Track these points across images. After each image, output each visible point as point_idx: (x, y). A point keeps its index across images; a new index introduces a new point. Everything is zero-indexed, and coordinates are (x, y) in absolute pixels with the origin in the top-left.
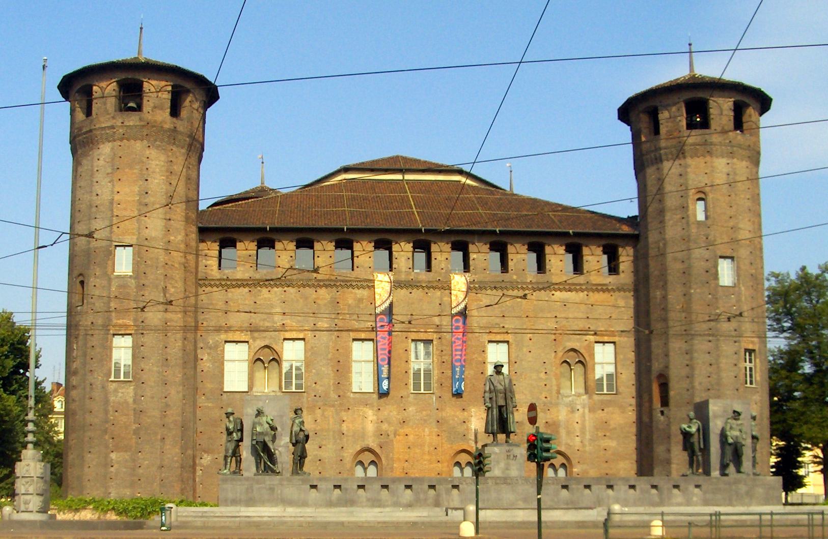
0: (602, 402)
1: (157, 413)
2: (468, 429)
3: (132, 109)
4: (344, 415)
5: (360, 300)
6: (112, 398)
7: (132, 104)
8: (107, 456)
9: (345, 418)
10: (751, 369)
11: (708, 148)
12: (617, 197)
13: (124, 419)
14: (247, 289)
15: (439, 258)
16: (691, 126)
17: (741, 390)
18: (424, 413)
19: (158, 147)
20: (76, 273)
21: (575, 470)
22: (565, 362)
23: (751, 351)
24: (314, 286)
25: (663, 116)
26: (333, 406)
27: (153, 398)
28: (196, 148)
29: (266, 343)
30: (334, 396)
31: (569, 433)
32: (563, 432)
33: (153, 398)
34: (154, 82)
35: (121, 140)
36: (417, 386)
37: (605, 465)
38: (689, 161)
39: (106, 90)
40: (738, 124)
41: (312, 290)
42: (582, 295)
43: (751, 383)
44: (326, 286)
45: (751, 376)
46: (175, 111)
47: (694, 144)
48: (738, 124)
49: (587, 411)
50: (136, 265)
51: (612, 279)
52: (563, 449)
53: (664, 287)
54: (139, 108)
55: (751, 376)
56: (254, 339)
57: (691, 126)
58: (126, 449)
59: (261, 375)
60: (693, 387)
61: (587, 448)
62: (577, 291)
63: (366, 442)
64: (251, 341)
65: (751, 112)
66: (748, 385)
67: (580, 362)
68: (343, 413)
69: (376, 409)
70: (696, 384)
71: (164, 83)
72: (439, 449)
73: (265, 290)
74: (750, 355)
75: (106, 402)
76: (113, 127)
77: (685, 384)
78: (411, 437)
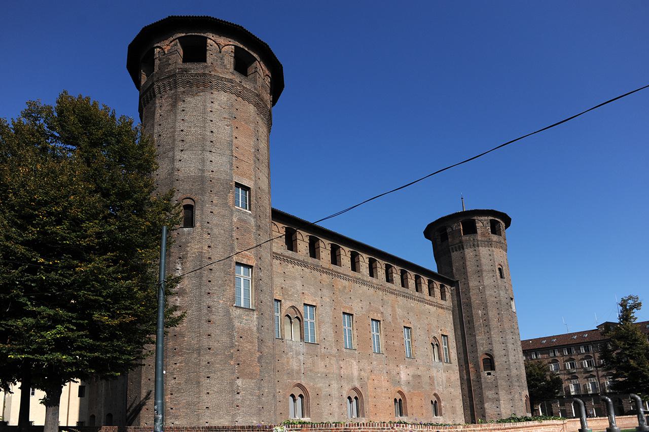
2: (400, 378)
4: (342, 364)
5: (345, 287)
9: (342, 366)
14: (278, 261)
21: (442, 404)
22: (432, 343)
24: (320, 271)
30: (334, 351)
31: (438, 383)
32: (436, 382)
41: (319, 273)
42: (435, 308)
44: (326, 273)
51: (443, 302)
52: (436, 392)
64: (283, 301)
68: (341, 362)
69: (357, 361)
72: (389, 390)
73: (290, 266)
78: (376, 381)
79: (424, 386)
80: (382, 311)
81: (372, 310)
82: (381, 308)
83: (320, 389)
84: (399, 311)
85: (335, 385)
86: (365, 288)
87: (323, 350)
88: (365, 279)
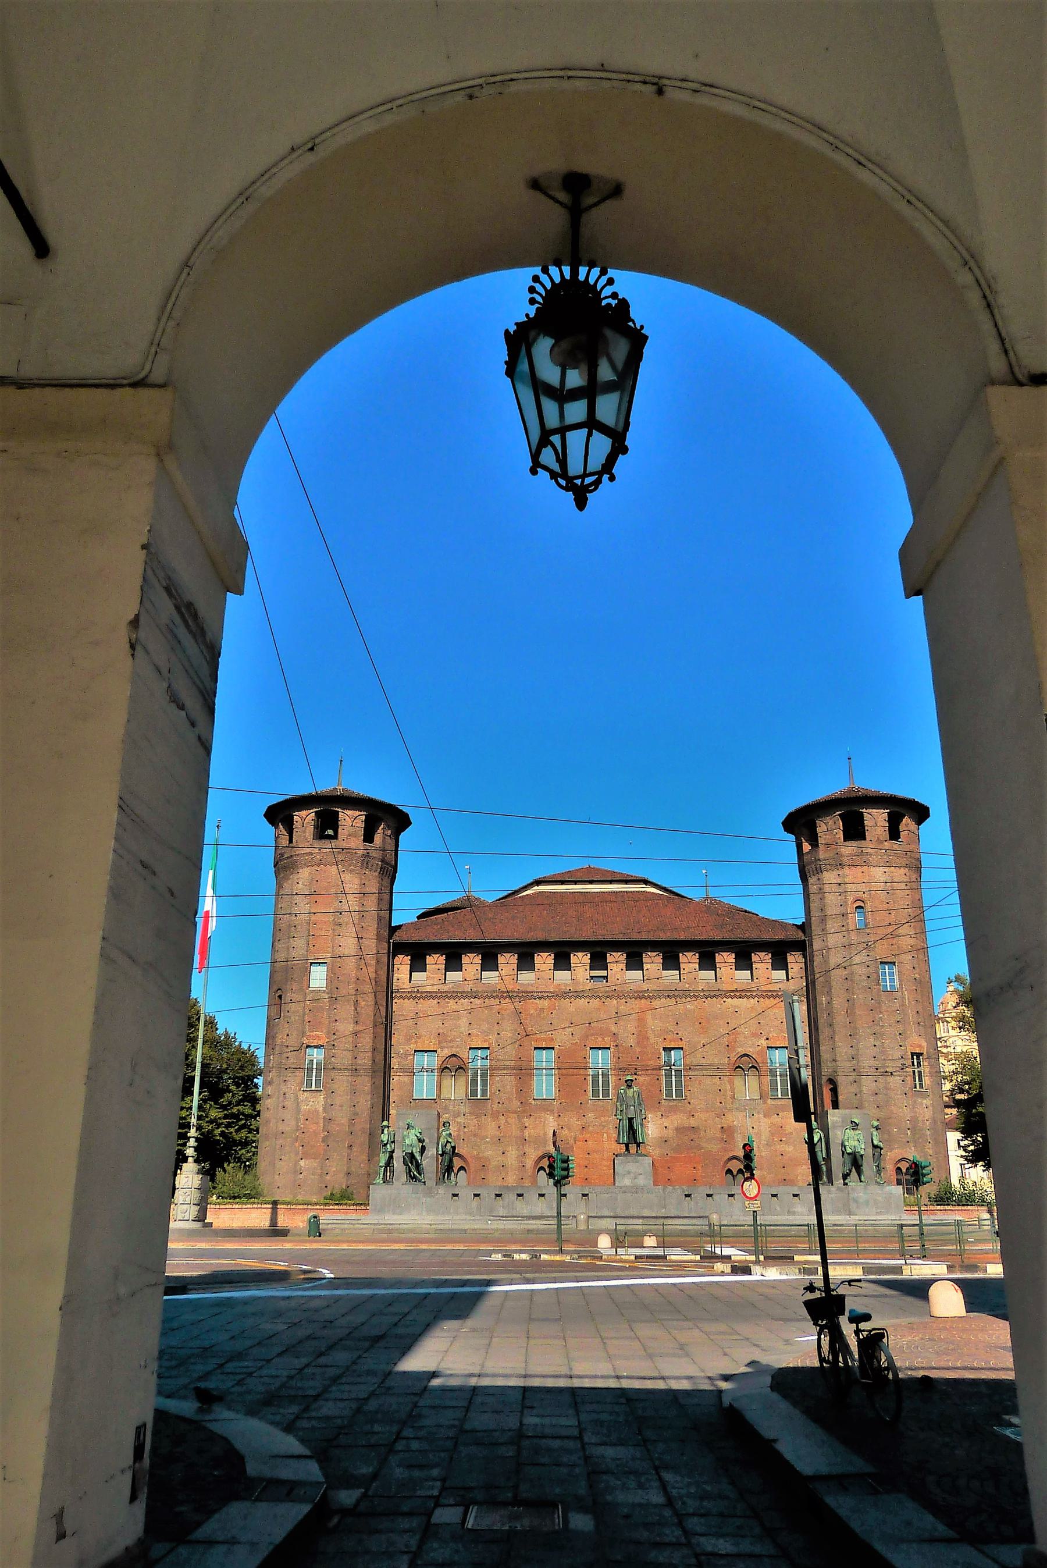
0: (776, 1106)
1: (344, 1121)
3: (329, 837)
4: (526, 1121)
5: (542, 1010)
6: (303, 1107)
7: (330, 832)
8: (296, 1163)
10: (920, 1073)
11: (865, 858)
12: (785, 908)
13: (314, 1127)
15: (615, 969)
16: (847, 838)
17: (910, 1094)
18: (603, 1119)
19: (352, 871)
20: (275, 988)
23: (919, 1055)
25: (821, 827)
26: (516, 1112)
27: (341, 1106)
28: (389, 871)
29: (454, 1051)
30: (516, 1103)
33: (341, 1106)
34: (349, 812)
35: (319, 865)
36: (595, 1093)
37: (783, 1170)
38: (847, 870)
39: (305, 819)
40: (894, 834)
41: (497, 1001)
43: (921, 1086)
45: (920, 1080)
46: (369, 837)
47: (850, 855)
48: (894, 834)
49: (761, 1116)
50: (329, 980)
53: (829, 993)
54: (335, 837)
55: (920, 1080)
56: (442, 1048)
57: (847, 838)
58: (315, 1157)
59: (448, 1082)
60: (861, 1092)
61: (763, 1154)
62: (748, 997)
63: (548, 1148)
64: (439, 1050)
65: (907, 823)
66: (918, 1089)
67: (753, 1067)
69: (556, 1115)
70: (864, 1088)
71: (358, 813)
73: (452, 1001)
74: (918, 1059)
75: (298, 1110)
76: (311, 854)
77: (853, 1089)
78: (590, 1143)
79: (704, 1145)
80: (616, 1031)
81: (592, 1035)
82: (614, 1029)
83: (488, 1159)
84: (654, 1024)
85: (513, 1153)
86: (582, 1002)
87: (495, 1106)
88: (581, 988)
